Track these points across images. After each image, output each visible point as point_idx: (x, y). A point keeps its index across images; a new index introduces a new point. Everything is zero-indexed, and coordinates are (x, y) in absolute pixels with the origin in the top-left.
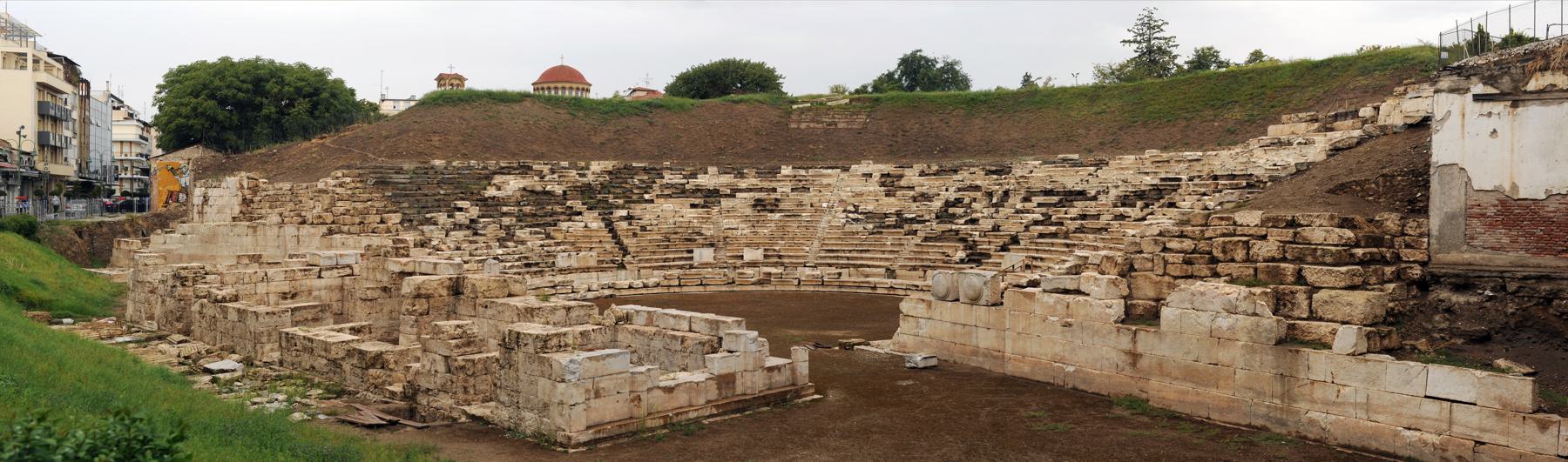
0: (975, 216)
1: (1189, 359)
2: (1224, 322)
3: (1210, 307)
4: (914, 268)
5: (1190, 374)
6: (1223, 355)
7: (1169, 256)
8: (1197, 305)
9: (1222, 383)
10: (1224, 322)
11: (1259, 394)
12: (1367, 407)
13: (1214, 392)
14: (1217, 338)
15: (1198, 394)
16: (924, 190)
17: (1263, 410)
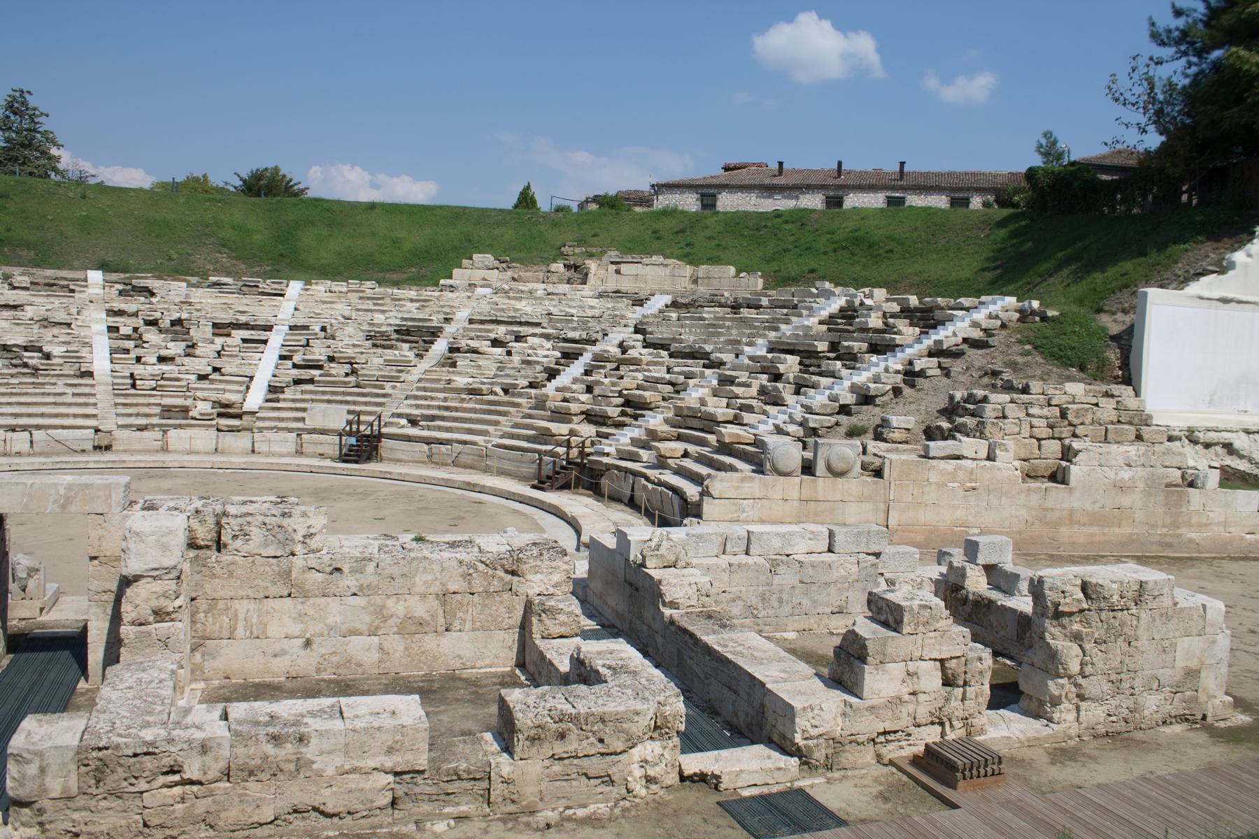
0: (164, 353)
1: (1096, 507)
2: (1126, 474)
3: (1114, 463)
4: (142, 428)
5: (1097, 519)
6: (1125, 501)
7: (1035, 421)
8: (1103, 462)
9: (1123, 523)
10: (1126, 474)
11: (1153, 526)
12: (1225, 524)
13: (1117, 530)
14: (1120, 487)
15: (1104, 534)
16: (42, 312)
17: (1157, 538)
